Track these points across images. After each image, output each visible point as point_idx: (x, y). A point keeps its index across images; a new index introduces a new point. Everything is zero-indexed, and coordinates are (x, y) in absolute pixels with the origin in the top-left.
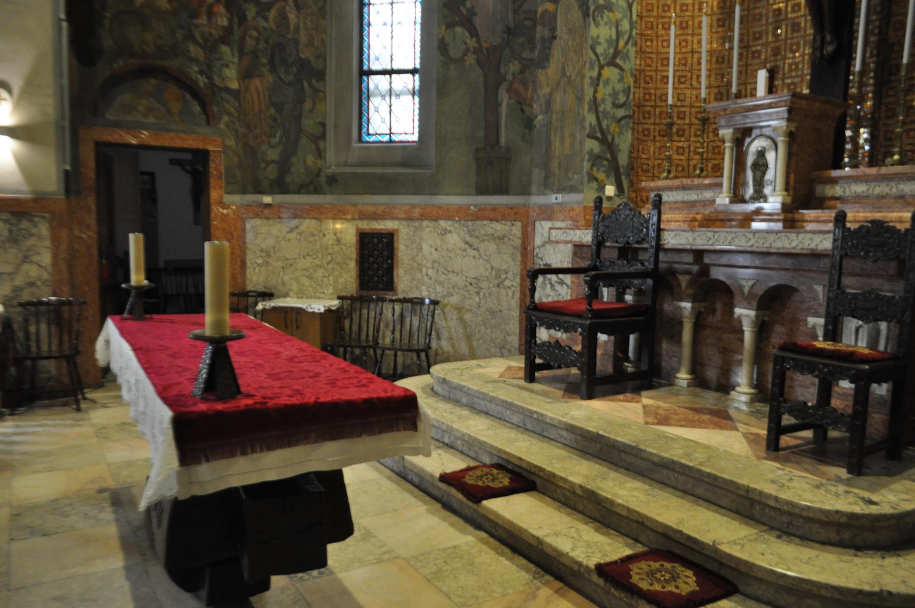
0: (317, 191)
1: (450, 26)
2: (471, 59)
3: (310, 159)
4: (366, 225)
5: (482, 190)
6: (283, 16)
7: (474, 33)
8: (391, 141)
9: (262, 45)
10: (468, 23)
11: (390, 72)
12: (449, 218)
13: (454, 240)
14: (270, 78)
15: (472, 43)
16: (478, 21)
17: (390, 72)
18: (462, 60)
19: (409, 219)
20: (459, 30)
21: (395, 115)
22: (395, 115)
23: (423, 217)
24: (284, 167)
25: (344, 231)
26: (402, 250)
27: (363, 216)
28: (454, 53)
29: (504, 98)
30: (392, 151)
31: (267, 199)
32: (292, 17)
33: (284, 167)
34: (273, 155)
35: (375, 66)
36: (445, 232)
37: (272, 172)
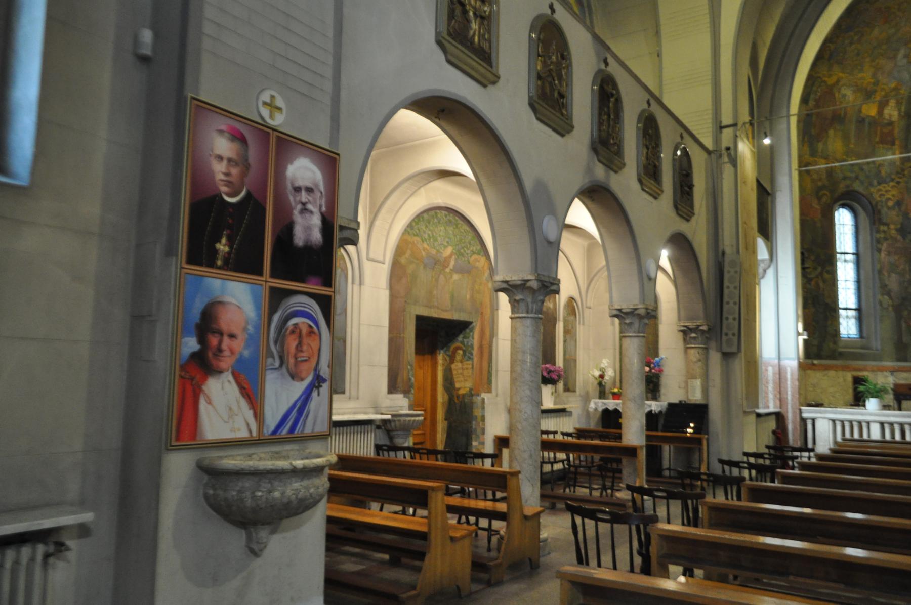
0: (834, 358)
1: (883, 295)
2: (890, 309)
3: (831, 345)
5: (898, 360)
6: (817, 285)
7: (891, 298)
10: (888, 294)
11: (846, 309)
14: (813, 310)
15: (890, 302)
16: (892, 294)
17: (846, 309)
18: (887, 308)
19: (873, 371)
20: (886, 297)
25: (849, 376)
28: (885, 306)
29: (904, 325)
30: (850, 342)
31: (815, 362)
32: (821, 285)
36: (886, 377)
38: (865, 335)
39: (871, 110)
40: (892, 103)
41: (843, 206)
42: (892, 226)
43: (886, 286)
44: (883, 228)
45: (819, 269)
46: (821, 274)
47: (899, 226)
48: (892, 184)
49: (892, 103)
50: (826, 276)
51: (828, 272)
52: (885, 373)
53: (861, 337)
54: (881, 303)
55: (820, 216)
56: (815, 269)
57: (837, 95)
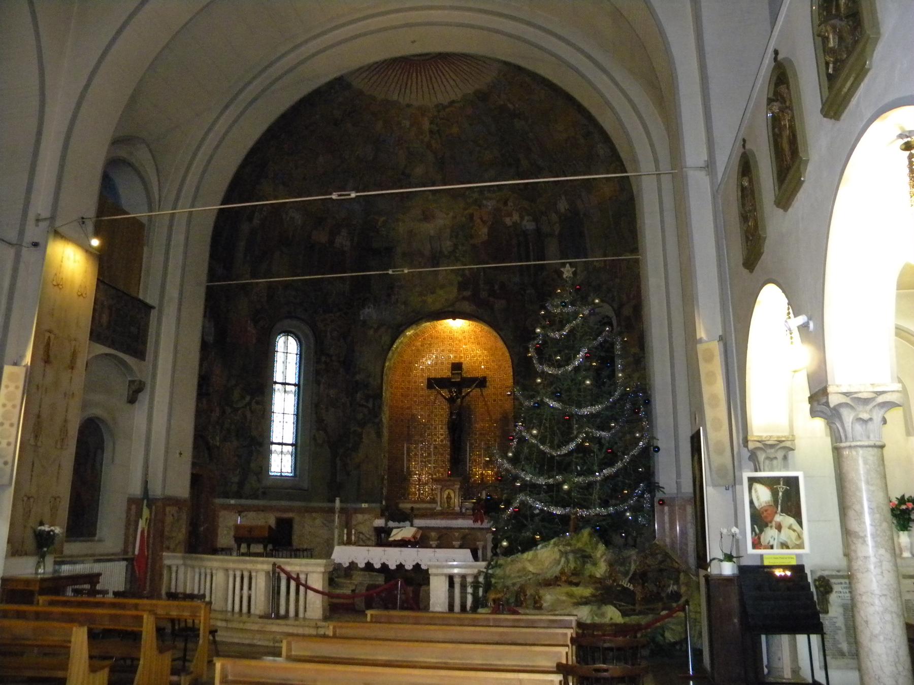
0: (256, 498)
4: (279, 515)
8: (281, 476)
9: (233, 427)
11: (282, 444)
12: (316, 512)
13: (318, 522)
17: (282, 444)
21: (281, 463)
22: (281, 463)
23: (307, 511)
24: (241, 484)
26: (296, 527)
27: (279, 510)
29: (338, 461)
31: (233, 502)
32: (249, 415)
33: (241, 484)
34: (236, 479)
35: (275, 441)
36: (315, 519)
37: (235, 488)
38: (298, 473)
39: (321, 237)
40: (344, 232)
41: (287, 333)
42: (334, 358)
43: (323, 420)
44: (323, 359)
45: (248, 398)
46: (249, 404)
47: (342, 359)
48: (338, 314)
49: (344, 232)
50: (254, 406)
51: (257, 403)
52: (314, 515)
53: (295, 476)
54: (315, 439)
55: (254, 341)
56: (243, 398)
57: (284, 216)
